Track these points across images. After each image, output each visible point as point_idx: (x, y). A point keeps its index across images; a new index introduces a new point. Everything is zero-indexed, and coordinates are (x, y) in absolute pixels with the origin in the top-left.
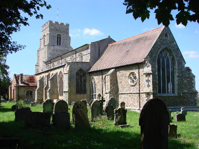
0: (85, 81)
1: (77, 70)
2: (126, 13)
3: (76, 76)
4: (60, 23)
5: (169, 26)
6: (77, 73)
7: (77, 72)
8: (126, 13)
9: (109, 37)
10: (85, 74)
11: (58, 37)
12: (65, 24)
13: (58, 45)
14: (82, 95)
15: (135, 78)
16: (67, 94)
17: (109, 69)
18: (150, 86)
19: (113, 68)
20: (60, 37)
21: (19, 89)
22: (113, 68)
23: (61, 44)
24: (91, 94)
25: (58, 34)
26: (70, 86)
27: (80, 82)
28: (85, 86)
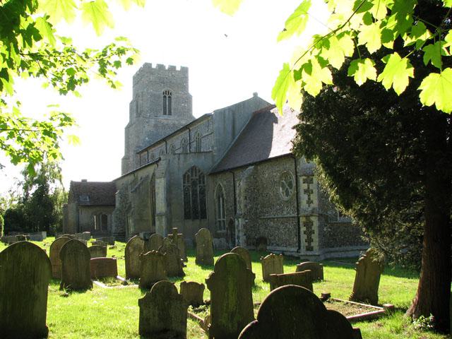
0: (203, 192)
1: (185, 171)
2: (310, 74)
3: (184, 183)
4: (178, 69)
5: (354, 47)
6: (184, 176)
7: (186, 173)
8: (310, 74)
9: (255, 94)
10: (204, 177)
11: (165, 97)
12: (178, 69)
13: (165, 113)
14: (197, 222)
15: (290, 185)
16: (164, 220)
17: (247, 166)
18: (312, 202)
19: (250, 165)
20: (169, 97)
21: (80, 211)
22: (250, 165)
23: (172, 111)
24: (218, 220)
25: (163, 90)
26: (169, 203)
27: (193, 194)
28: (203, 202)
